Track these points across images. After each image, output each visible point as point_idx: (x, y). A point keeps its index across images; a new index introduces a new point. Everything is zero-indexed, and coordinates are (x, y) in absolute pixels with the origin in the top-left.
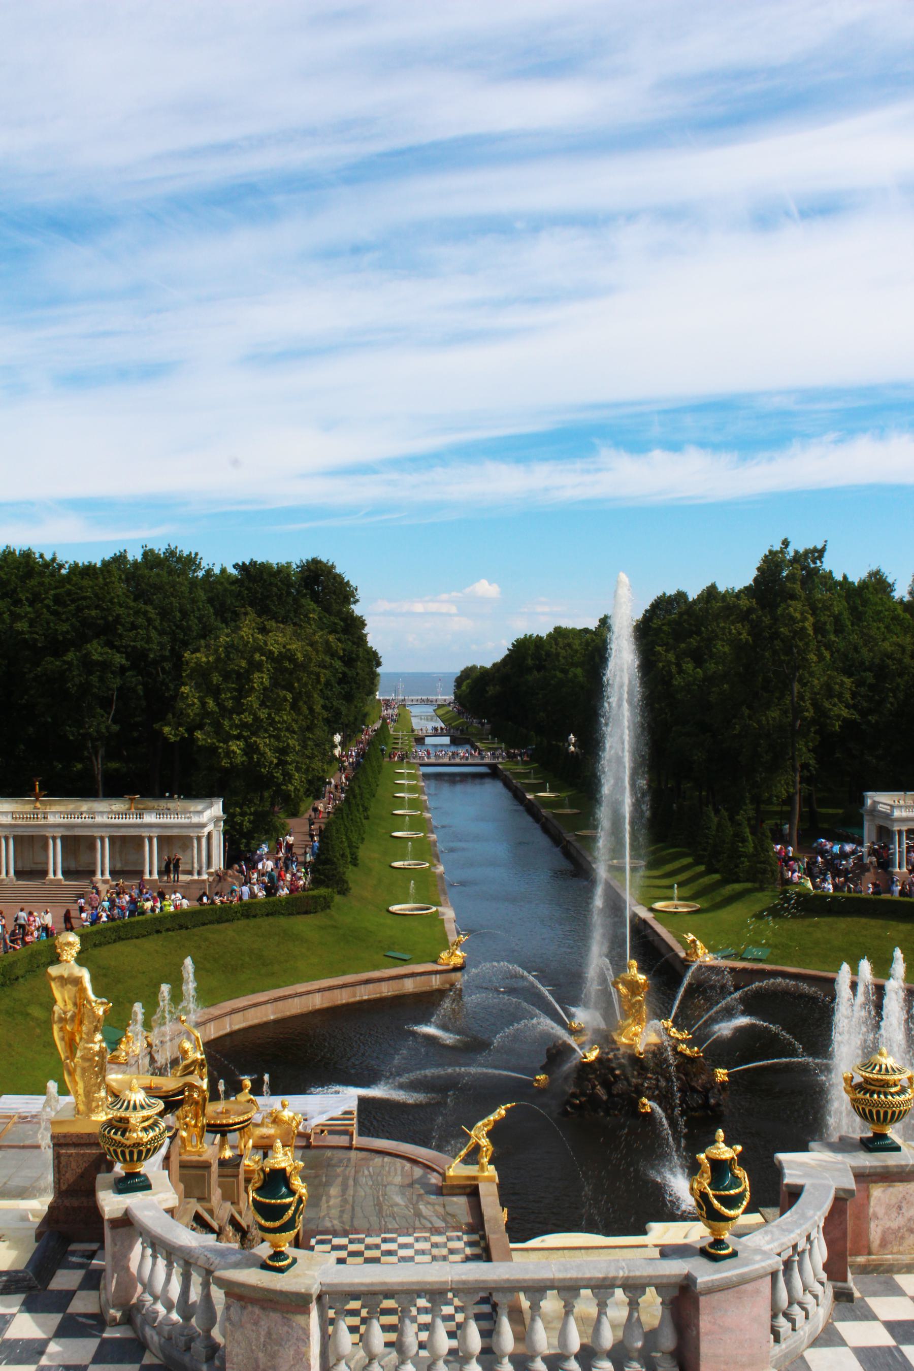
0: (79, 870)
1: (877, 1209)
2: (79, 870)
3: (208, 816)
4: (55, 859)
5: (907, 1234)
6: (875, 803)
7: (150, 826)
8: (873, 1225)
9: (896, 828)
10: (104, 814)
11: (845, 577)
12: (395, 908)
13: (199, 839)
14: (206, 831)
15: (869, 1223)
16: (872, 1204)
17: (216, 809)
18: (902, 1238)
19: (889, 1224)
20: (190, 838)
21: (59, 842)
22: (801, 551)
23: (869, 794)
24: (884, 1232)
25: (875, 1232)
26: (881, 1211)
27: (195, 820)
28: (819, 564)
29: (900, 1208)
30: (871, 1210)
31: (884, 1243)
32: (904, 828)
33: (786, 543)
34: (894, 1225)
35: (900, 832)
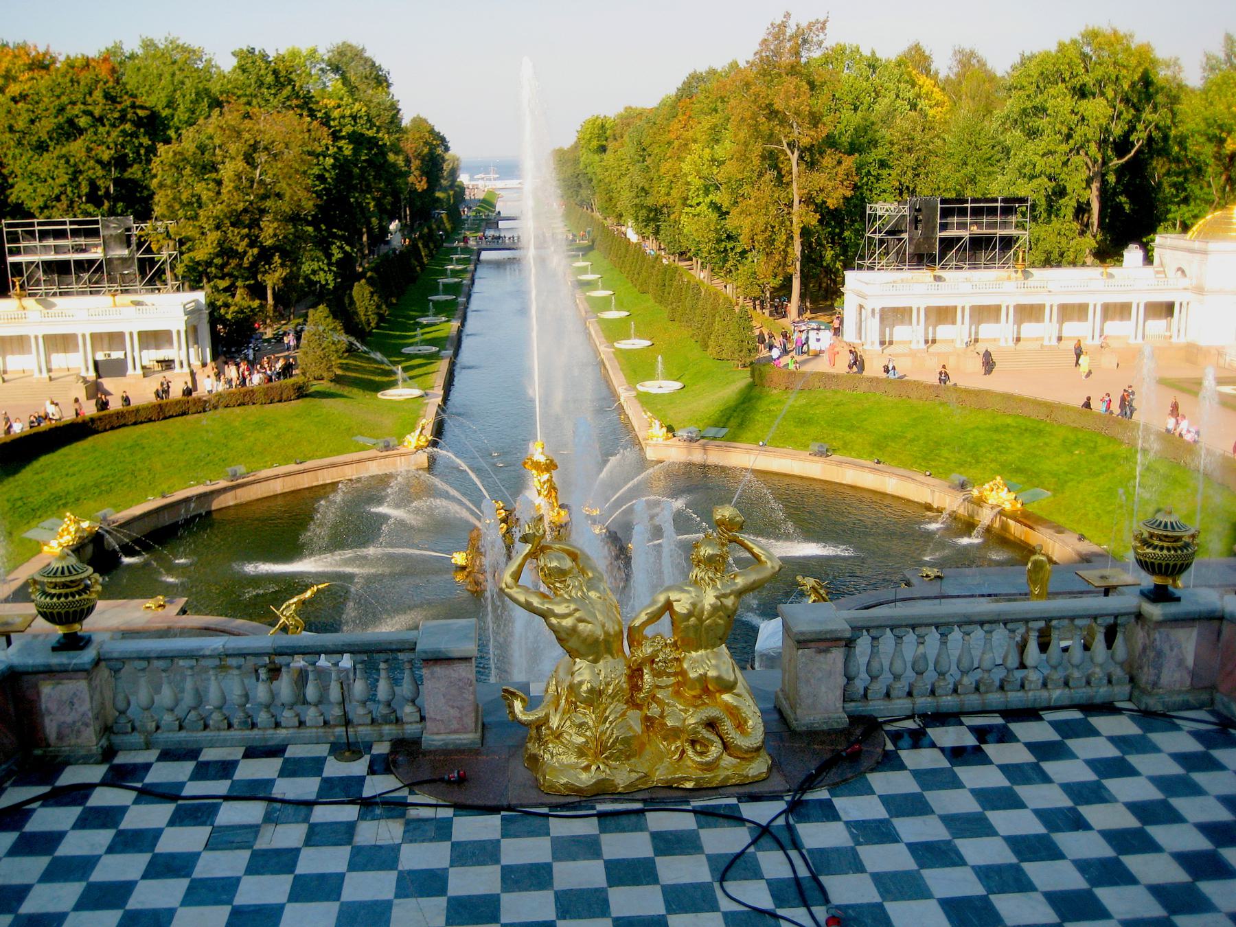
1: (49, 705)
5: (83, 728)
8: (47, 721)
11: (873, 53)
15: (42, 716)
16: (44, 698)
18: (79, 731)
19: (62, 719)
22: (804, 24)
24: (59, 726)
25: (51, 727)
26: (53, 707)
28: (822, 36)
29: (72, 704)
30: (43, 707)
31: (60, 737)
33: (788, 15)
34: (69, 719)
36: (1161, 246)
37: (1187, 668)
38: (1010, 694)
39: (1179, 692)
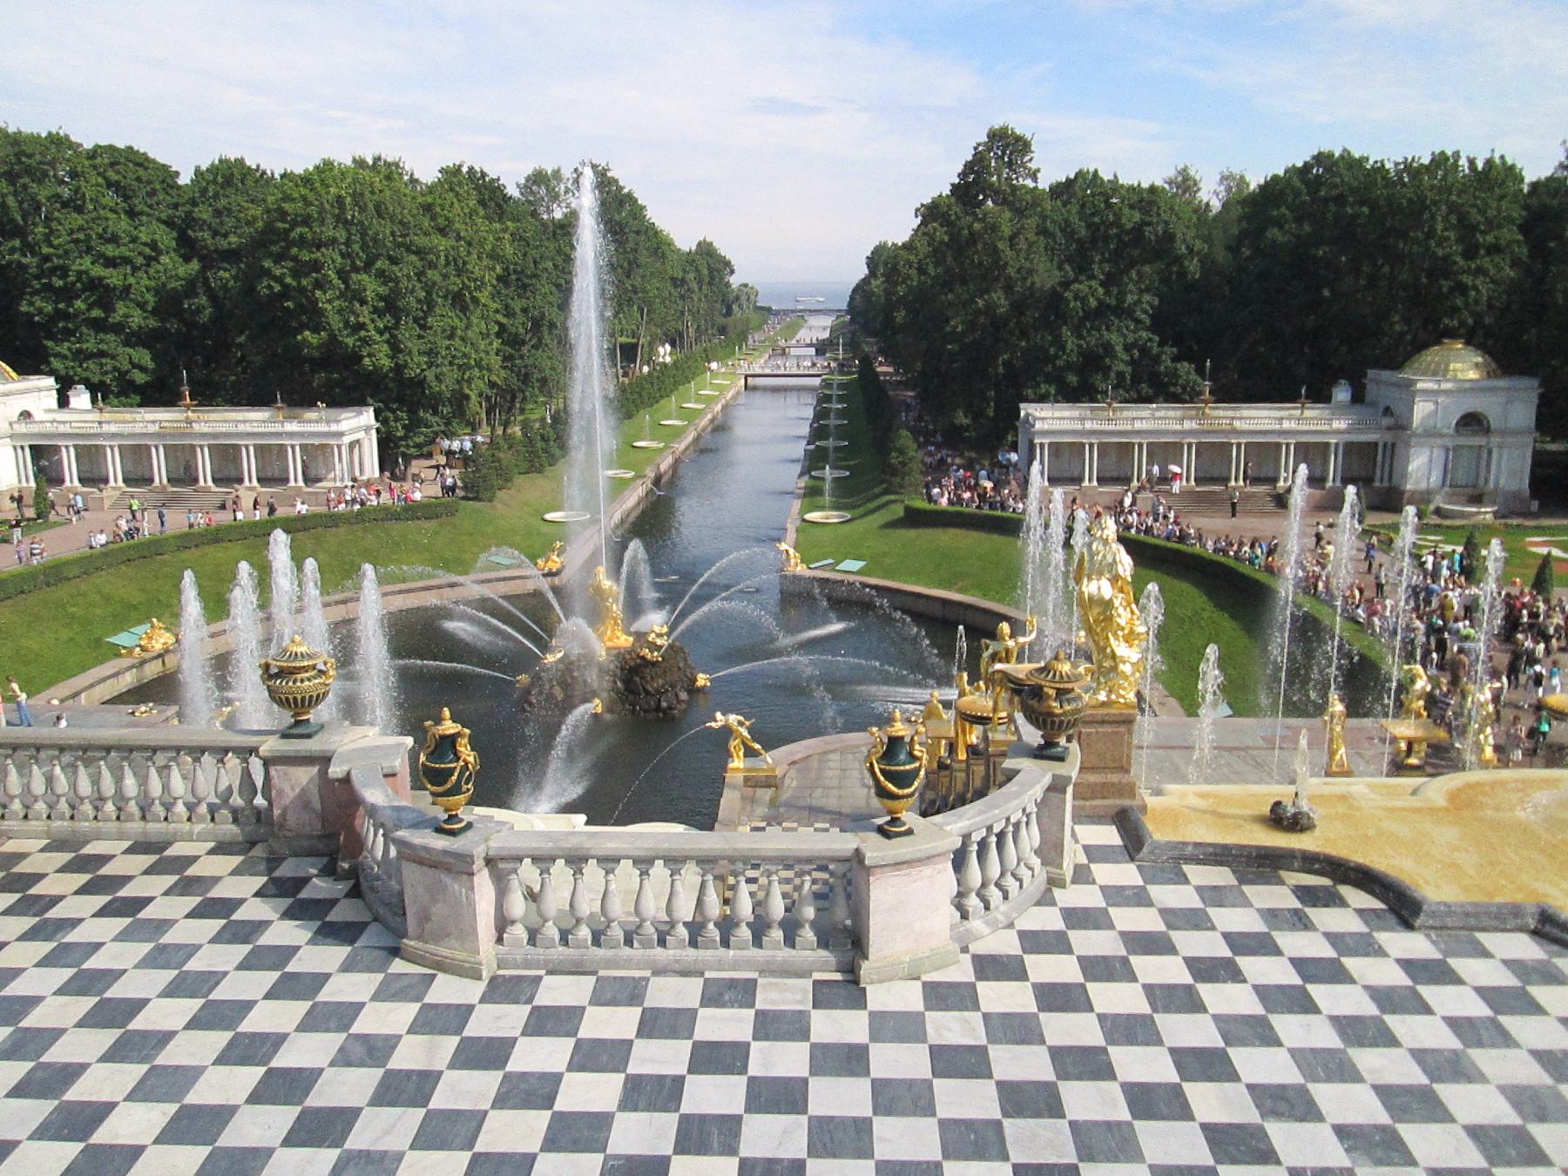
0: (228, 477)
2: (228, 477)
3: (357, 426)
4: (205, 466)
6: (1028, 415)
7: (291, 435)
9: (1037, 441)
10: (249, 423)
12: (548, 516)
13: (339, 447)
14: (346, 440)
17: (367, 417)
20: (331, 447)
21: (206, 450)
23: (1022, 406)
27: (334, 428)
32: (1046, 441)
35: (1042, 445)
36: (1372, 380)
37: (314, 810)
38: (151, 825)
39: (311, 837)
